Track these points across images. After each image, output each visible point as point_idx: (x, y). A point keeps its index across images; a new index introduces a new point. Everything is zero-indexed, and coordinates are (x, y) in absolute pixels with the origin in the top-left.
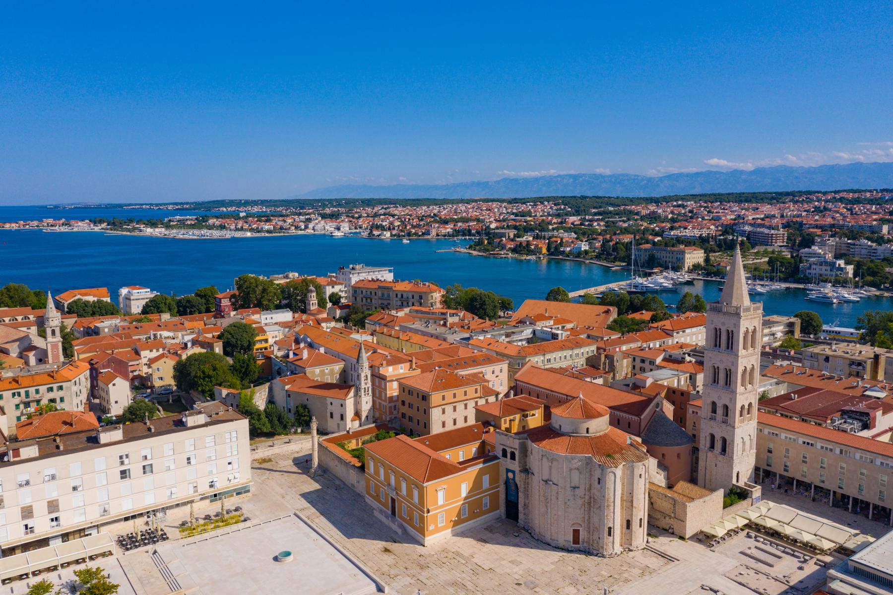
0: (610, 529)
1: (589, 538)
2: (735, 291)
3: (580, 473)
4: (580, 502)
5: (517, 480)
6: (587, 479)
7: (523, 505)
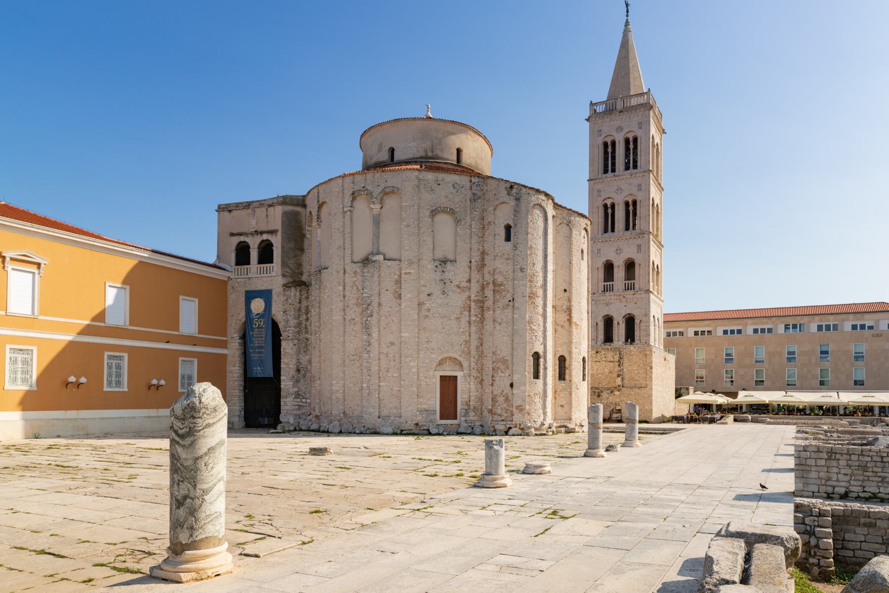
0: (536, 356)
1: (481, 400)
2: (631, 81)
3: (457, 221)
4: (457, 300)
5: (277, 312)
6: (475, 239)
7: (293, 372)
